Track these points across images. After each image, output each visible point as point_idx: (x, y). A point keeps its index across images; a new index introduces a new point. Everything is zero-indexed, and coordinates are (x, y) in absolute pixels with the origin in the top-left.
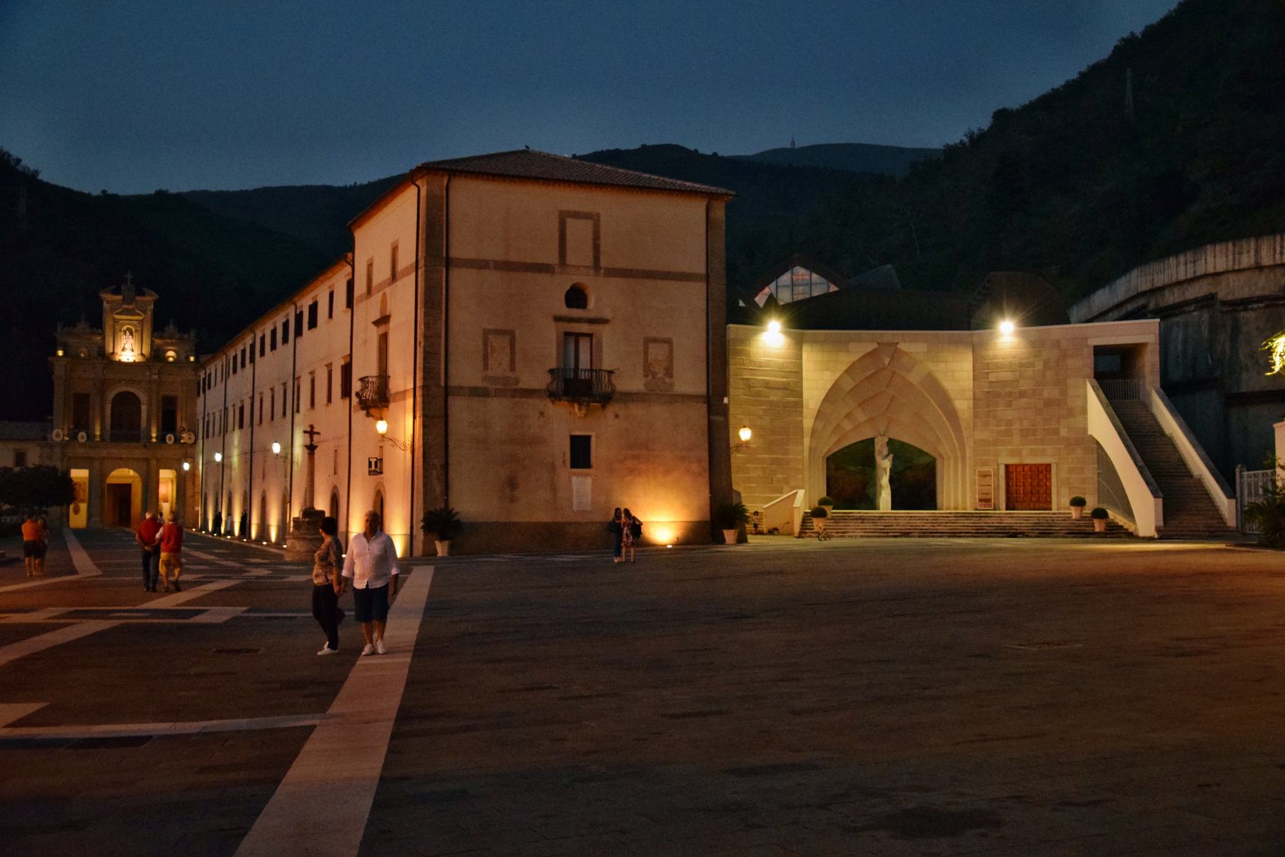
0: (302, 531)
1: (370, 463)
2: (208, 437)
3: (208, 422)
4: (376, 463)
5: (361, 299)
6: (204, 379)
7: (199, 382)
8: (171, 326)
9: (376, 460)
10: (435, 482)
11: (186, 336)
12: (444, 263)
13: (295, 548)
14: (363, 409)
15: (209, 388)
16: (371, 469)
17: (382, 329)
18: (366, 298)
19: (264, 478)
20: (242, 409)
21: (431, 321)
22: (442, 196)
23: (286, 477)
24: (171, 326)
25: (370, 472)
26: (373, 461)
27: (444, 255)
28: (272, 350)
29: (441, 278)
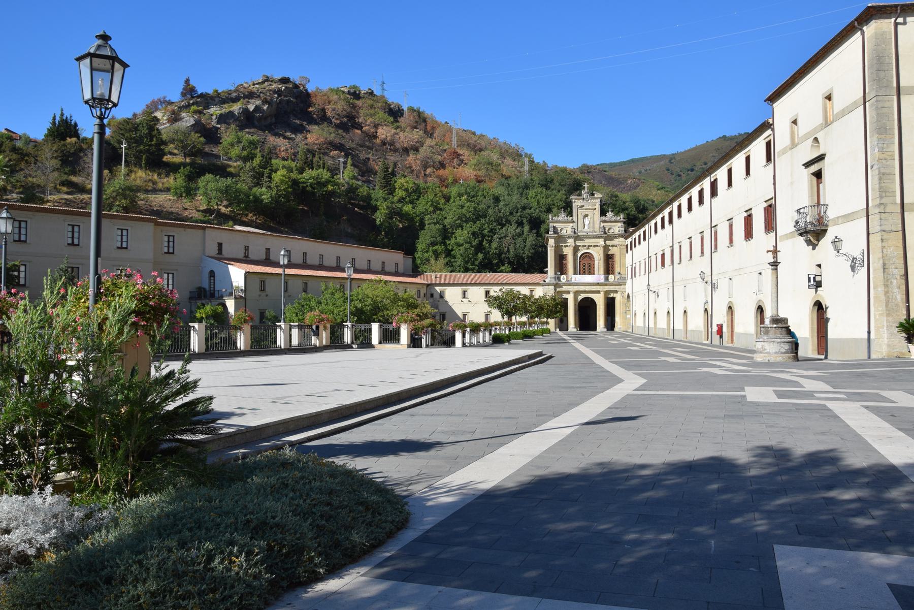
0: (771, 336)
1: (809, 279)
2: (635, 276)
3: (635, 267)
4: (814, 278)
5: (784, 151)
6: (631, 243)
7: (627, 246)
8: (610, 213)
9: (814, 276)
10: (896, 290)
11: (618, 218)
12: (895, 91)
13: (766, 349)
14: (801, 235)
15: (635, 246)
16: (810, 284)
17: (814, 168)
18: (791, 149)
19: (685, 298)
20: (663, 255)
21: (885, 145)
22: (890, 32)
23: (706, 296)
24: (610, 213)
25: (809, 286)
26: (812, 277)
27: (895, 84)
28: (678, 217)
29: (892, 107)
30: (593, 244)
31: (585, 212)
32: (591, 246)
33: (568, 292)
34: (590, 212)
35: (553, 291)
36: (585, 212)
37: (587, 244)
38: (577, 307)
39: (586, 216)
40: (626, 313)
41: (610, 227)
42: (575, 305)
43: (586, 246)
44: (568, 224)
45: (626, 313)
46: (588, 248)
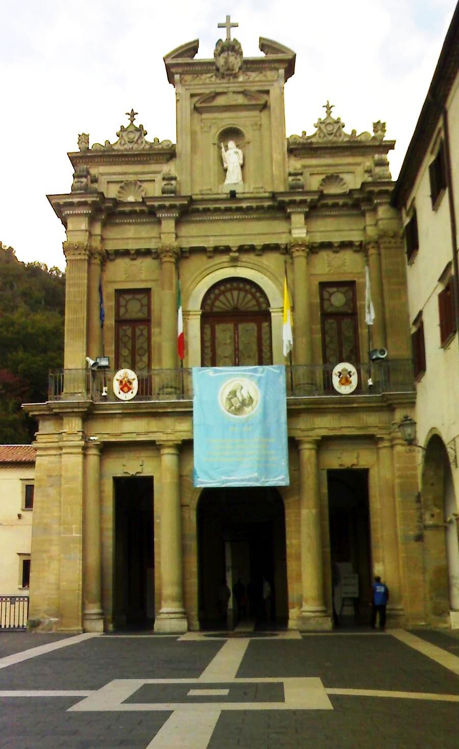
30: (258, 242)
31: (228, 120)
32: (251, 249)
33: (152, 446)
34: (242, 120)
35: (78, 441)
36: (228, 120)
37: (234, 243)
38: (192, 516)
39: (231, 133)
40: (419, 538)
41: (332, 171)
42: (182, 506)
43: (227, 250)
44: (154, 167)
45: (419, 538)
46: (234, 262)
